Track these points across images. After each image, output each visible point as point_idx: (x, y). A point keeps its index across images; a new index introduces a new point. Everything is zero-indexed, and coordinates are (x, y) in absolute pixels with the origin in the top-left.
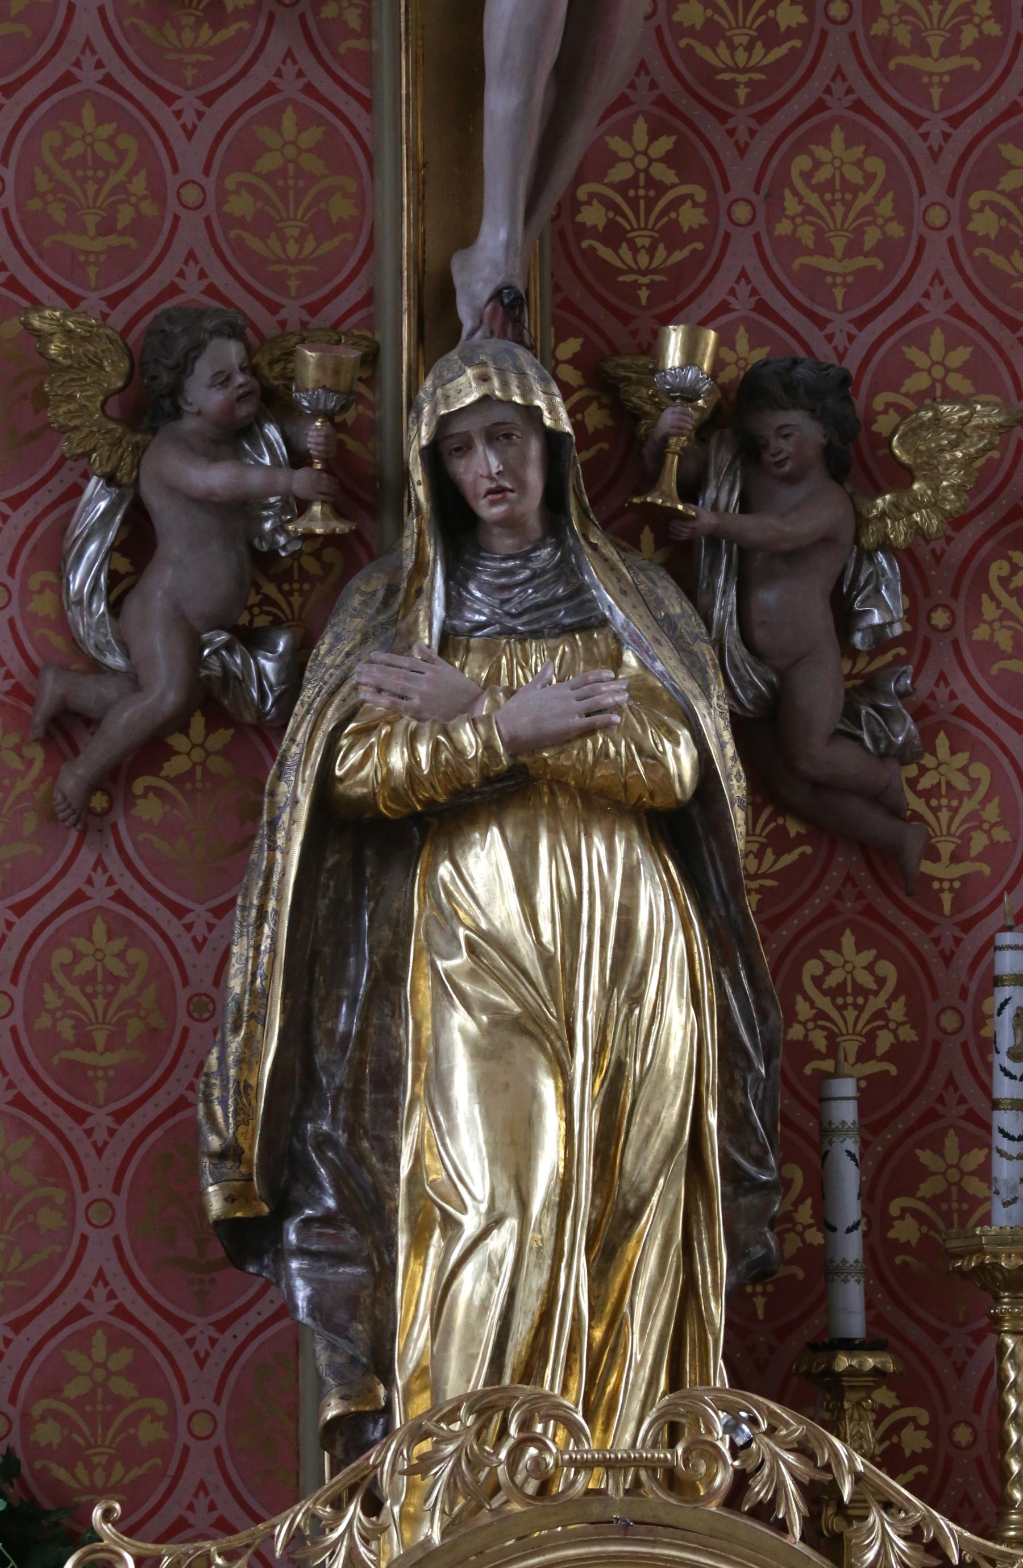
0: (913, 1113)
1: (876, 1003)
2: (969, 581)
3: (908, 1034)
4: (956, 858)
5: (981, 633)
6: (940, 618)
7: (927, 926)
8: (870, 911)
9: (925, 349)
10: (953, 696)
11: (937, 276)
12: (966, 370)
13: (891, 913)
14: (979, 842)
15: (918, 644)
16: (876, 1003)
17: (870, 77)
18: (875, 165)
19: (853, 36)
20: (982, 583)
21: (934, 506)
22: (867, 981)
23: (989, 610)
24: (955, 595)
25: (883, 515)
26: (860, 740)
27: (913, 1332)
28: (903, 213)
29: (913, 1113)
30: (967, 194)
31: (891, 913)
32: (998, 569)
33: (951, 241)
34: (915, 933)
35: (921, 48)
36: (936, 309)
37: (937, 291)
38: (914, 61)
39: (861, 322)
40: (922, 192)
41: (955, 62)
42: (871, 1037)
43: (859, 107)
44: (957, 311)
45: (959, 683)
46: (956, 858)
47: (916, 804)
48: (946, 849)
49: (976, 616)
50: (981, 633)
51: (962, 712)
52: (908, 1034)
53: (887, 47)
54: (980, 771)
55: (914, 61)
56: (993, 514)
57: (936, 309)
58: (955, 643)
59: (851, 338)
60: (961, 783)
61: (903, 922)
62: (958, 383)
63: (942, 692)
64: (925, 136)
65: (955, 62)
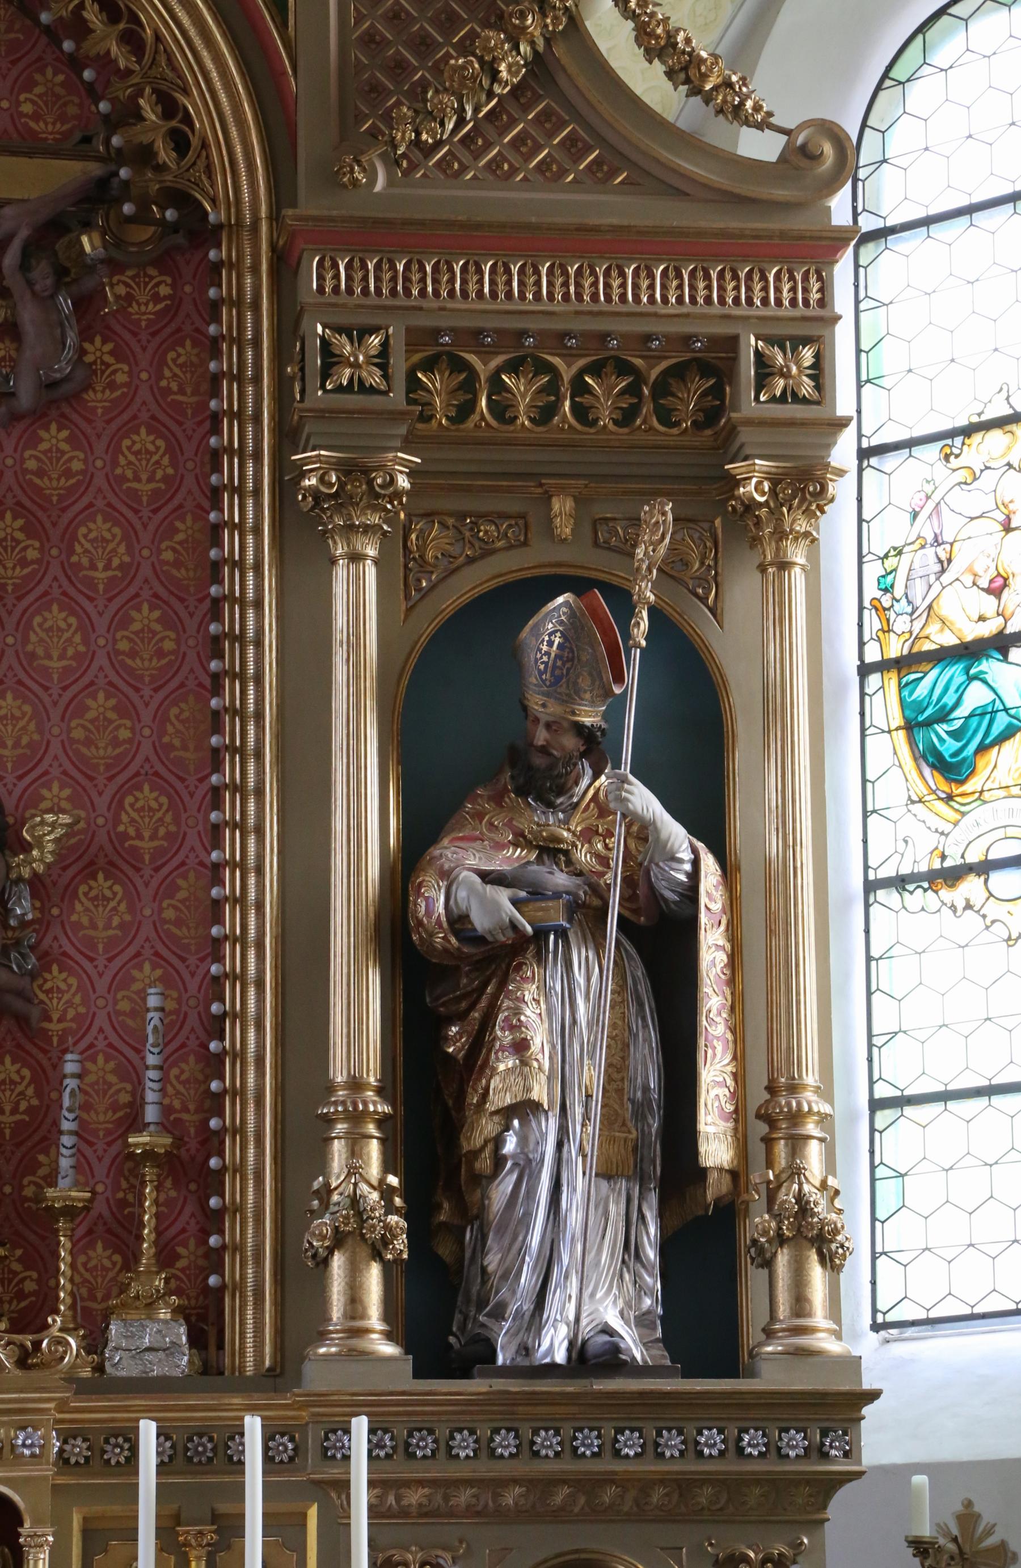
0: (36, 1138)
1: (20, 1088)
2: (69, 893)
3: (35, 1102)
4: (60, 1021)
5: (74, 918)
6: (55, 911)
7: (45, 1051)
8: (19, 1046)
9: (50, 790)
10: (61, 946)
11: (56, 757)
12: (68, 799)
13: (29, 1046)
14: (71, 1014)
15: (42, 923)
16: (20, 1088)
17: (24, 669)
18: (27, 708)
19: (17, 652)
20: (75, 895)
21: (41, 860)
22: (16, 1078)
23: (78, 907)
24: (62, 900)
25: (18, 865)
26: (11, 968)
27: (32, 1237)
28: (40, 731)
29: (36, 1138)
30: (70, 721)
31: (29, 1046)
32: (83, 889)
33: (62, 742)
34: (40, 1056)
35: (49, 657)
36: (55, 772)
37: (56, 764)
38: (46, 662)
39: (20, 778)
40: (49, 720)
41: (65, 663)
42: (17, 1104)
43: (20, 682)
44: (65, 773)
45: (64, 941)
46: (60, 1021)
47: (42, 996)
48: (55, 1017)
49: (72, 910)
50: (74, 918)
51: (65, 954)
52: (35, 1102)
53: (33, 656)
54: (73, 981)
55: (46, 662)
56: (81, 864)
57: (55, 772)
58: (62, 923)
59: (15, 785)
60: (63, 986)
61: (35, 1051)
62: (64, 804)
63: (55, 945)
64: (50, 695)
65: (65, 663)
